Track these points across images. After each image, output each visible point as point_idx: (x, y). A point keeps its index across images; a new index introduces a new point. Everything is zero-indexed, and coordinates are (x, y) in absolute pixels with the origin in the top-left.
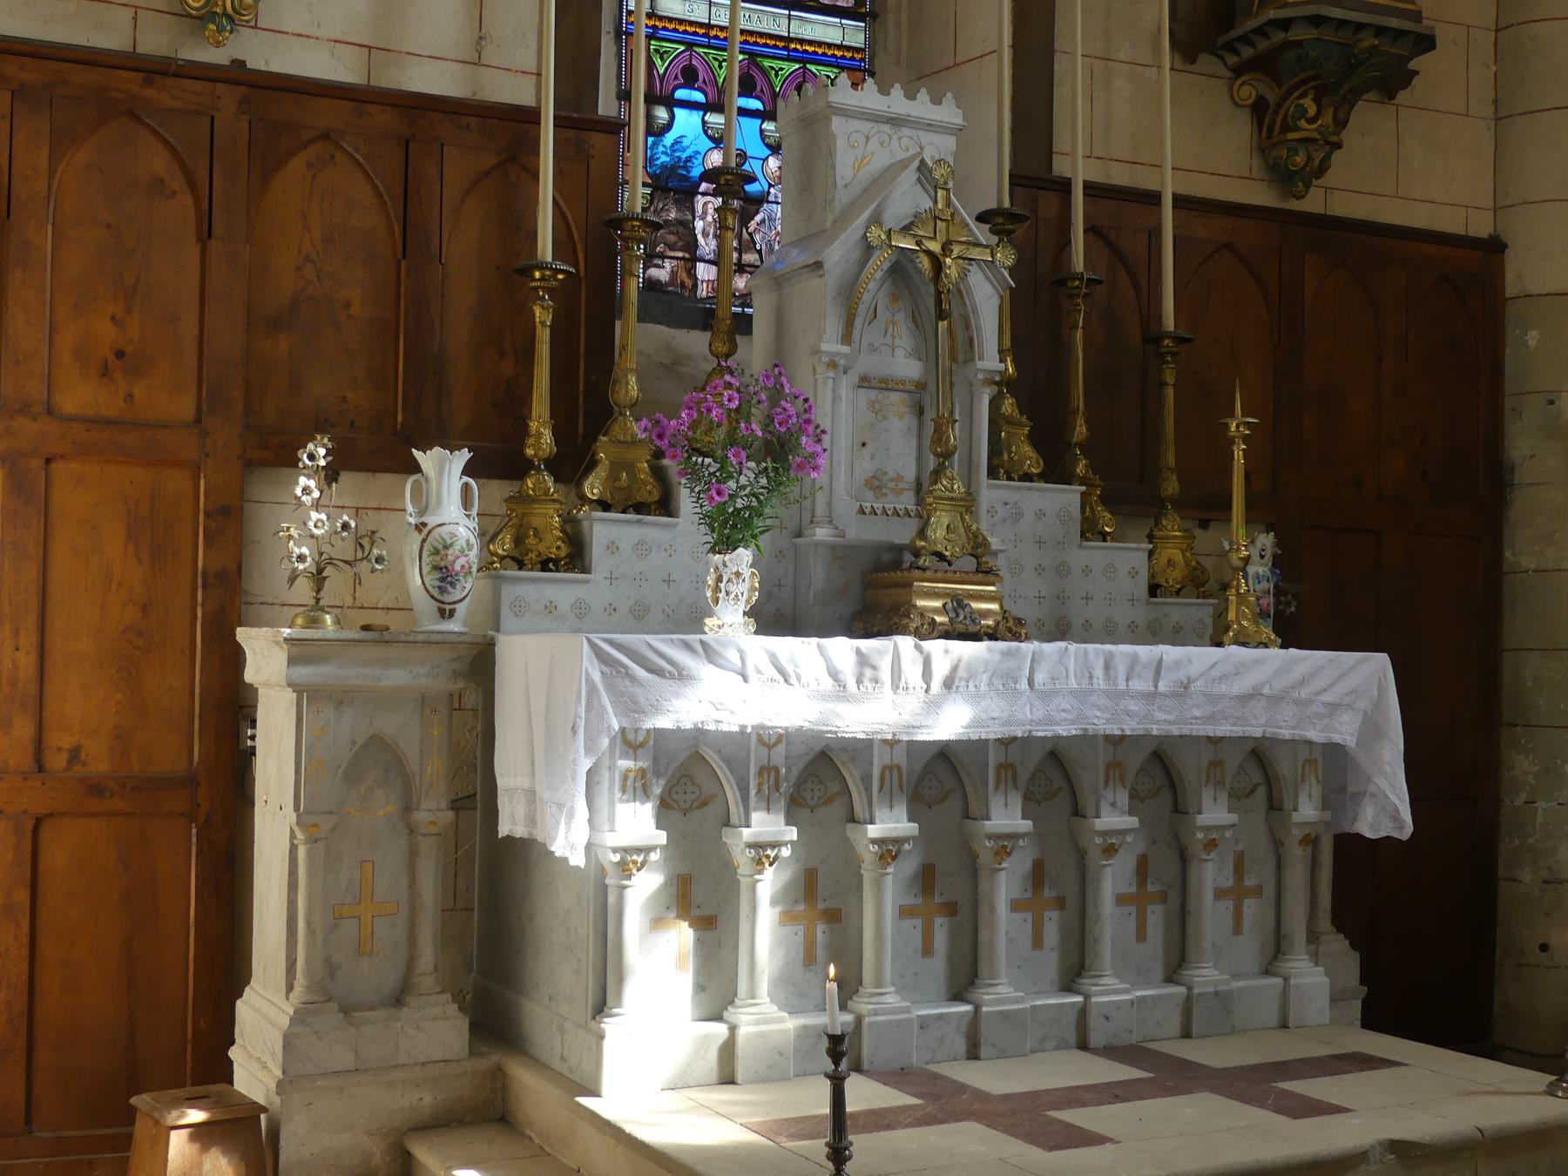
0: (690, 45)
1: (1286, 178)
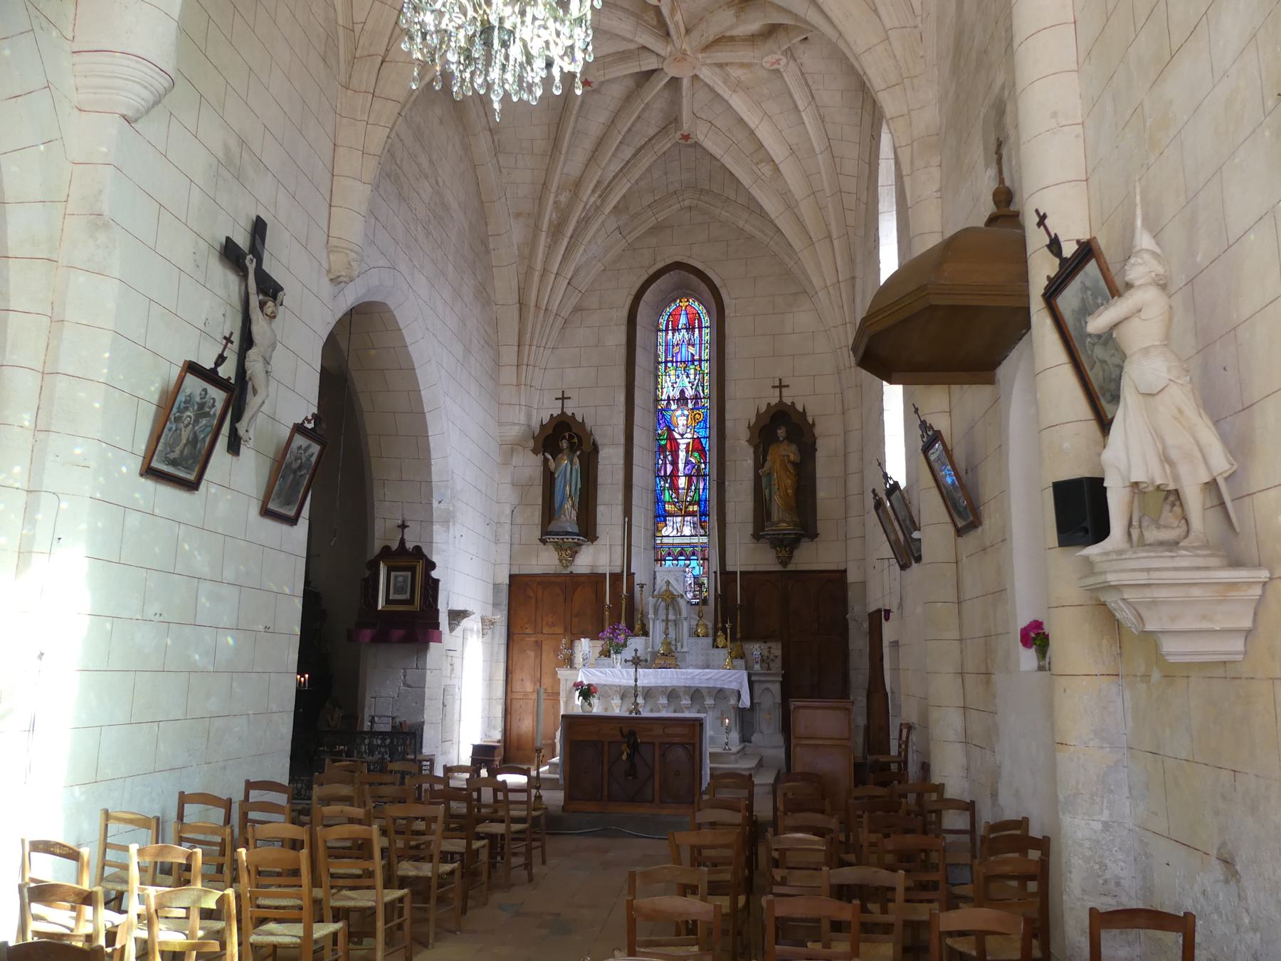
0: (669, 548)
1: (784, 563)
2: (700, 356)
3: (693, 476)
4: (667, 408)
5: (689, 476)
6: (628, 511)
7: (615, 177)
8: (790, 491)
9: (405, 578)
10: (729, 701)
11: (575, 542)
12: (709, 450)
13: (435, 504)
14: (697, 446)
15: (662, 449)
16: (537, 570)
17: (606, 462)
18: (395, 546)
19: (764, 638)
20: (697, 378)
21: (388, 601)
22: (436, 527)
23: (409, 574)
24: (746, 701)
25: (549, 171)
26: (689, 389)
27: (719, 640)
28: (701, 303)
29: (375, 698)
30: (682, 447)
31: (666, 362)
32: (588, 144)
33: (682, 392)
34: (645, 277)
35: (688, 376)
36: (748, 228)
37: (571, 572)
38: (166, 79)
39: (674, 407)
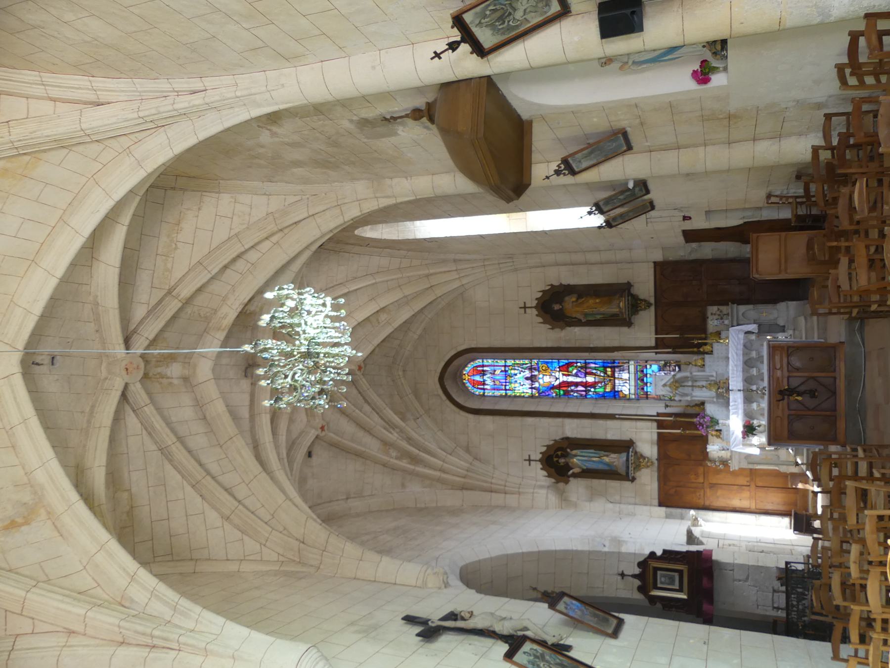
1: (649, 305)
2: (502, 366)
3: (586, 371)
4: (538, 389)
5: (586, 374)
6: (611, 417)
7: (382, 418)
8: (598, 301)
9: (662, 576)
10: (753, 340)
12: (568, 360)
13: (606, 549)
14: (565, 368)
15: (567, 393)
16: (655, 485)
18: (637, 583)
19: (704, 319)
20: (517, 368)
21: (680, 590)
22: (624, 549)
23: (659, 573)
24: (753, 327)
25: (376, 461)
26: (525, 373)
27: (706, 351)
28: (466, 366)
29: (758, 606)
30: (565, 379)
31: (506, 390)
32: (361, 434)
33: (527, 379)
34: (448, 403)
35: (516, 375)
36: (419, 332)
37: (657, 459)
38: (312, 650)
39: (537, 385)
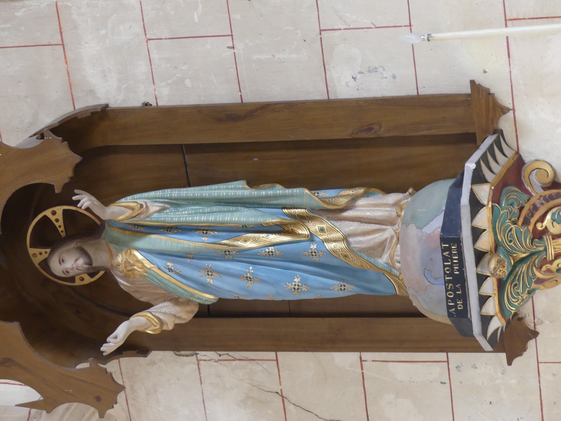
11: (496, 198)
17: (142, 68)
